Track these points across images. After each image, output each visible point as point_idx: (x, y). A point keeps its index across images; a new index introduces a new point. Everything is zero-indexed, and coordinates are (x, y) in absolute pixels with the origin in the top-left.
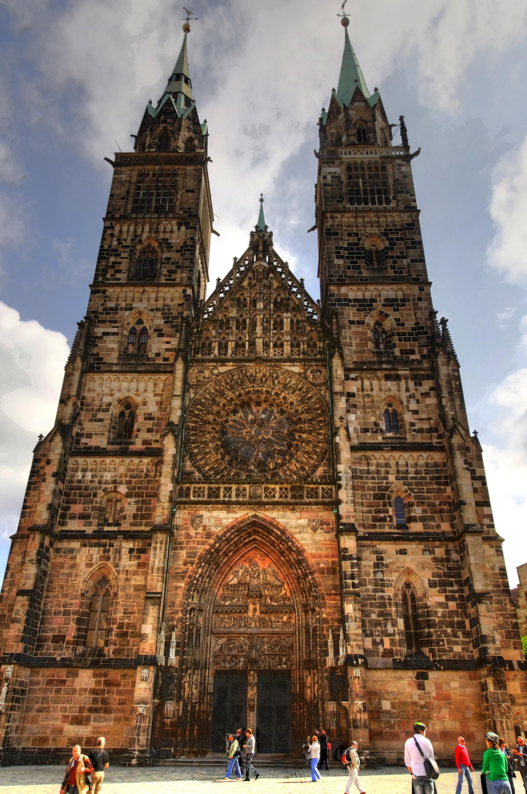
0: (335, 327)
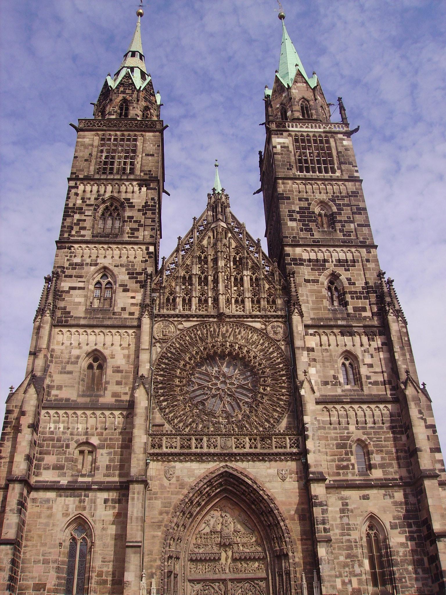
0: (293, 285)
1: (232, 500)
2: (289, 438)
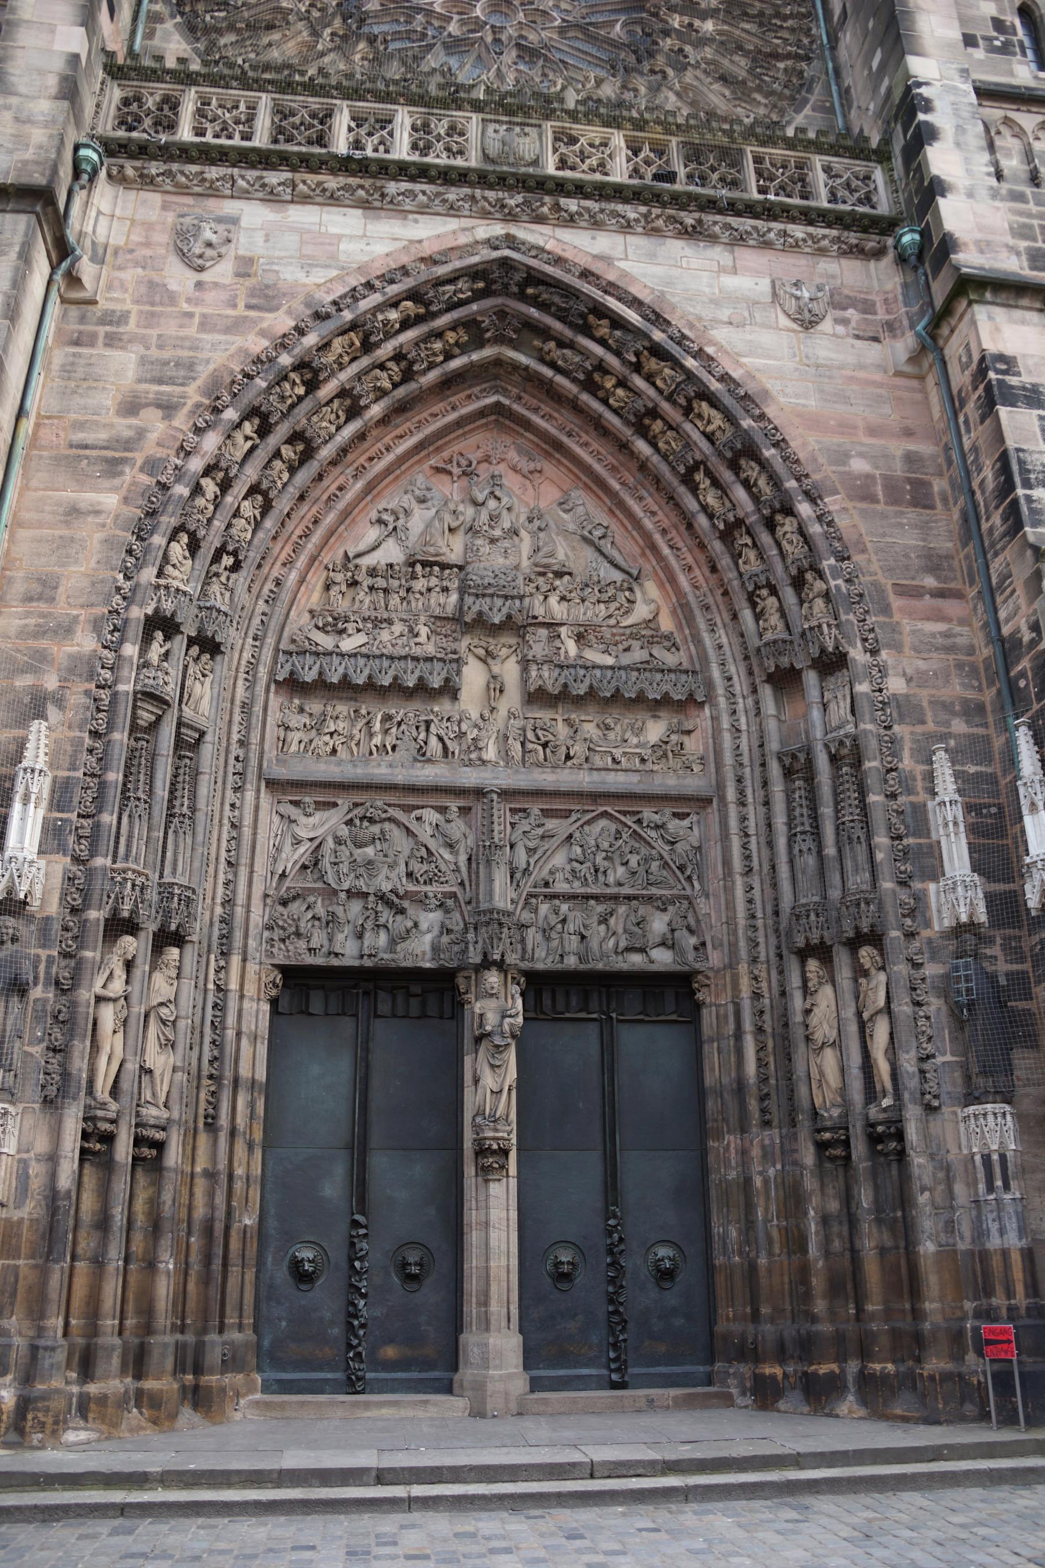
1: (527, 425)
2: (827, 169)
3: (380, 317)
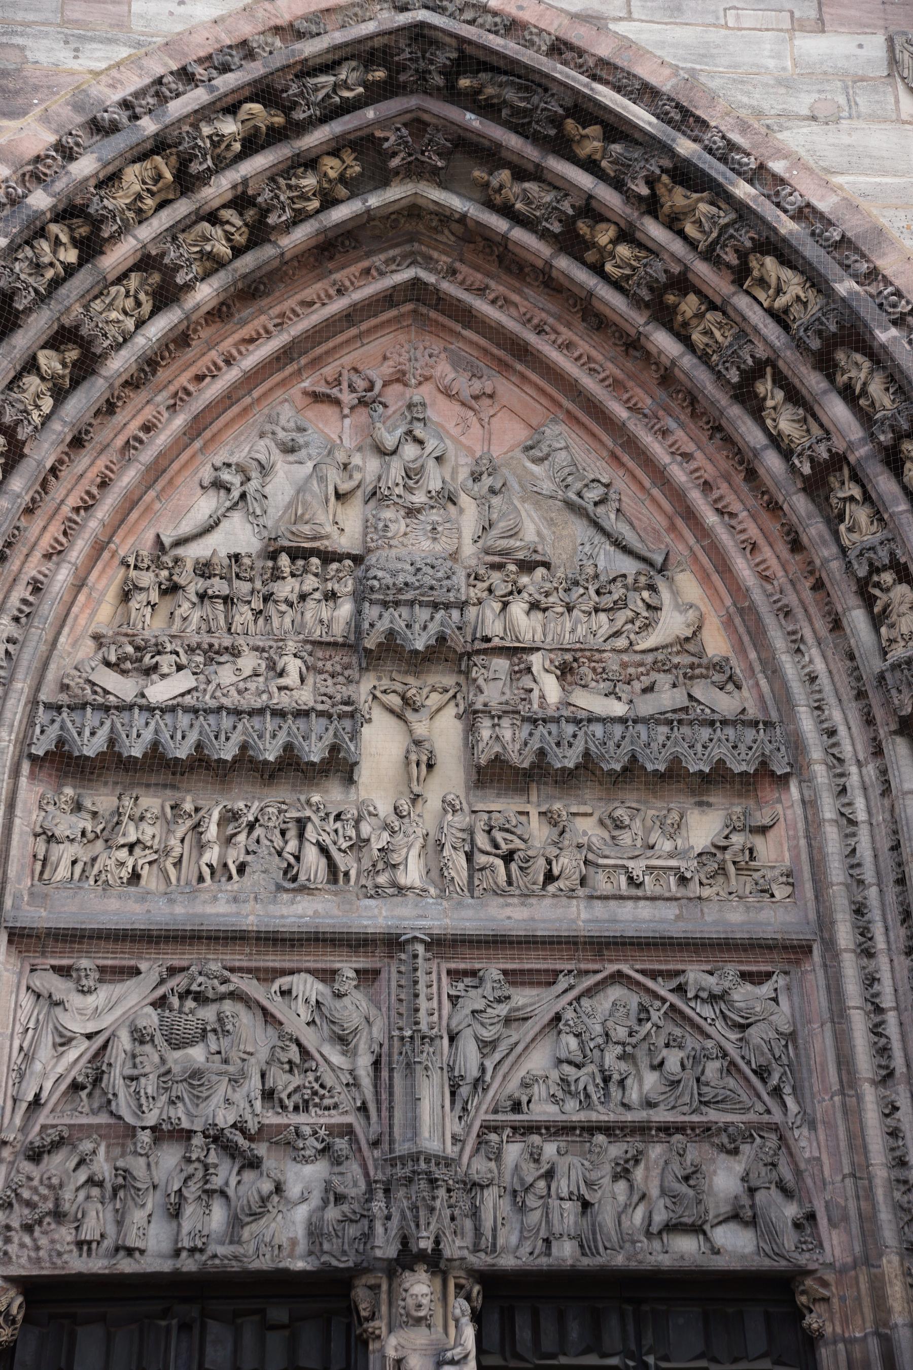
1: (467, 317)
3: (206, 130)
